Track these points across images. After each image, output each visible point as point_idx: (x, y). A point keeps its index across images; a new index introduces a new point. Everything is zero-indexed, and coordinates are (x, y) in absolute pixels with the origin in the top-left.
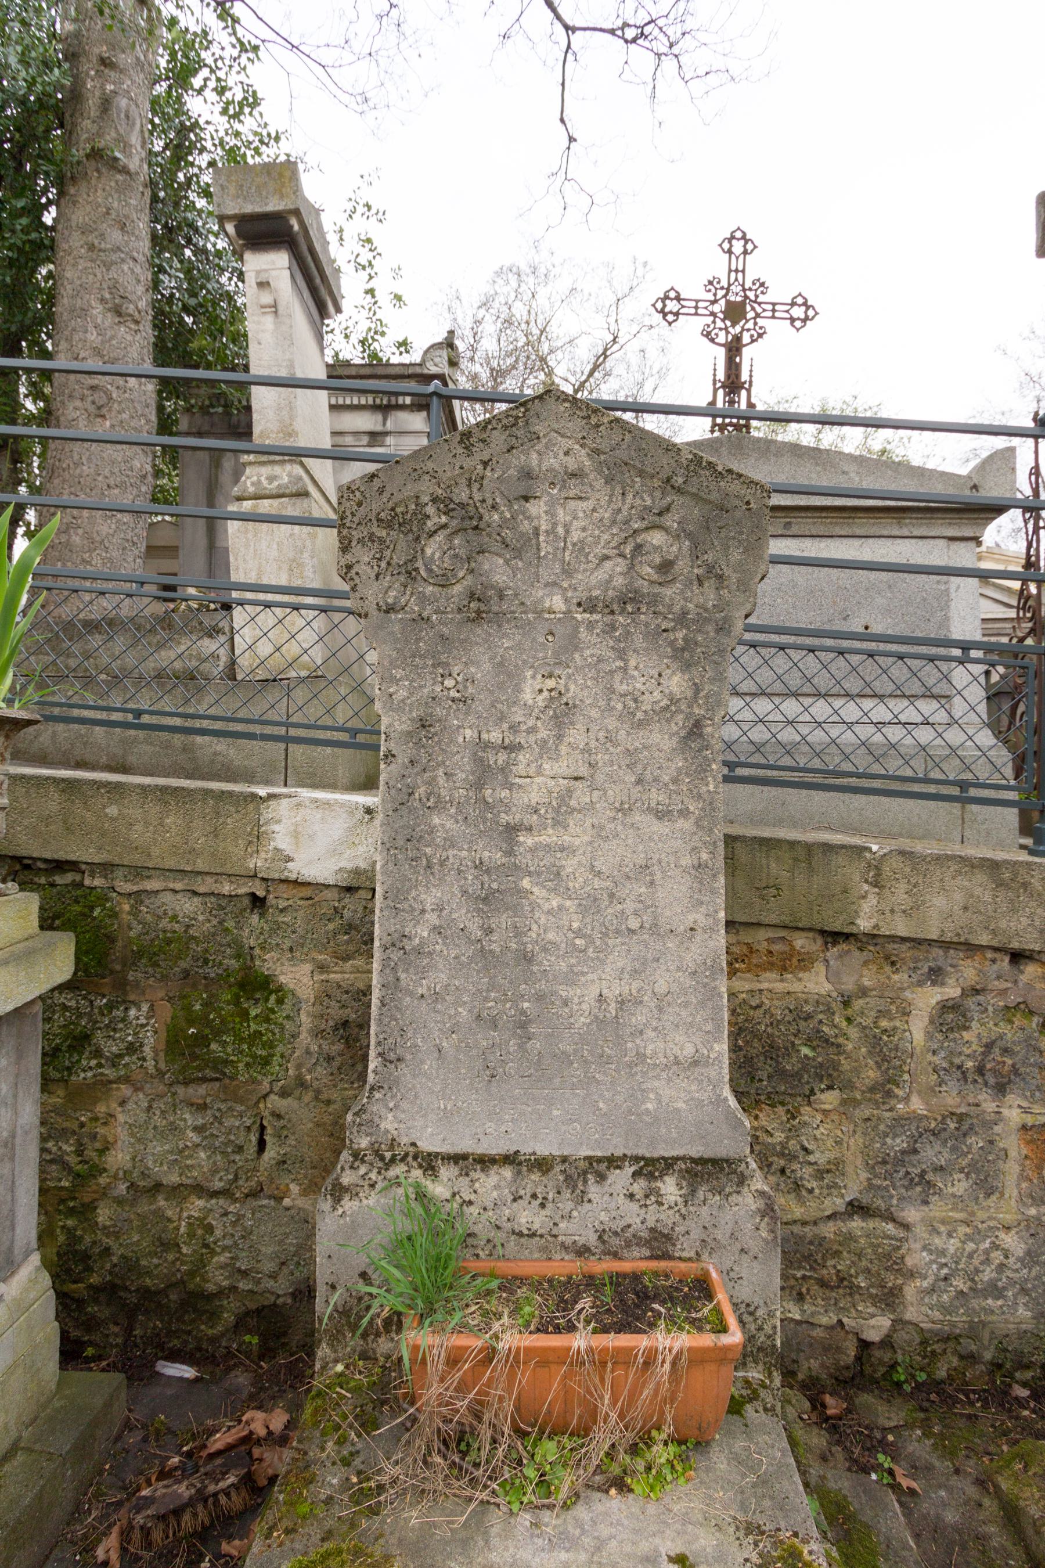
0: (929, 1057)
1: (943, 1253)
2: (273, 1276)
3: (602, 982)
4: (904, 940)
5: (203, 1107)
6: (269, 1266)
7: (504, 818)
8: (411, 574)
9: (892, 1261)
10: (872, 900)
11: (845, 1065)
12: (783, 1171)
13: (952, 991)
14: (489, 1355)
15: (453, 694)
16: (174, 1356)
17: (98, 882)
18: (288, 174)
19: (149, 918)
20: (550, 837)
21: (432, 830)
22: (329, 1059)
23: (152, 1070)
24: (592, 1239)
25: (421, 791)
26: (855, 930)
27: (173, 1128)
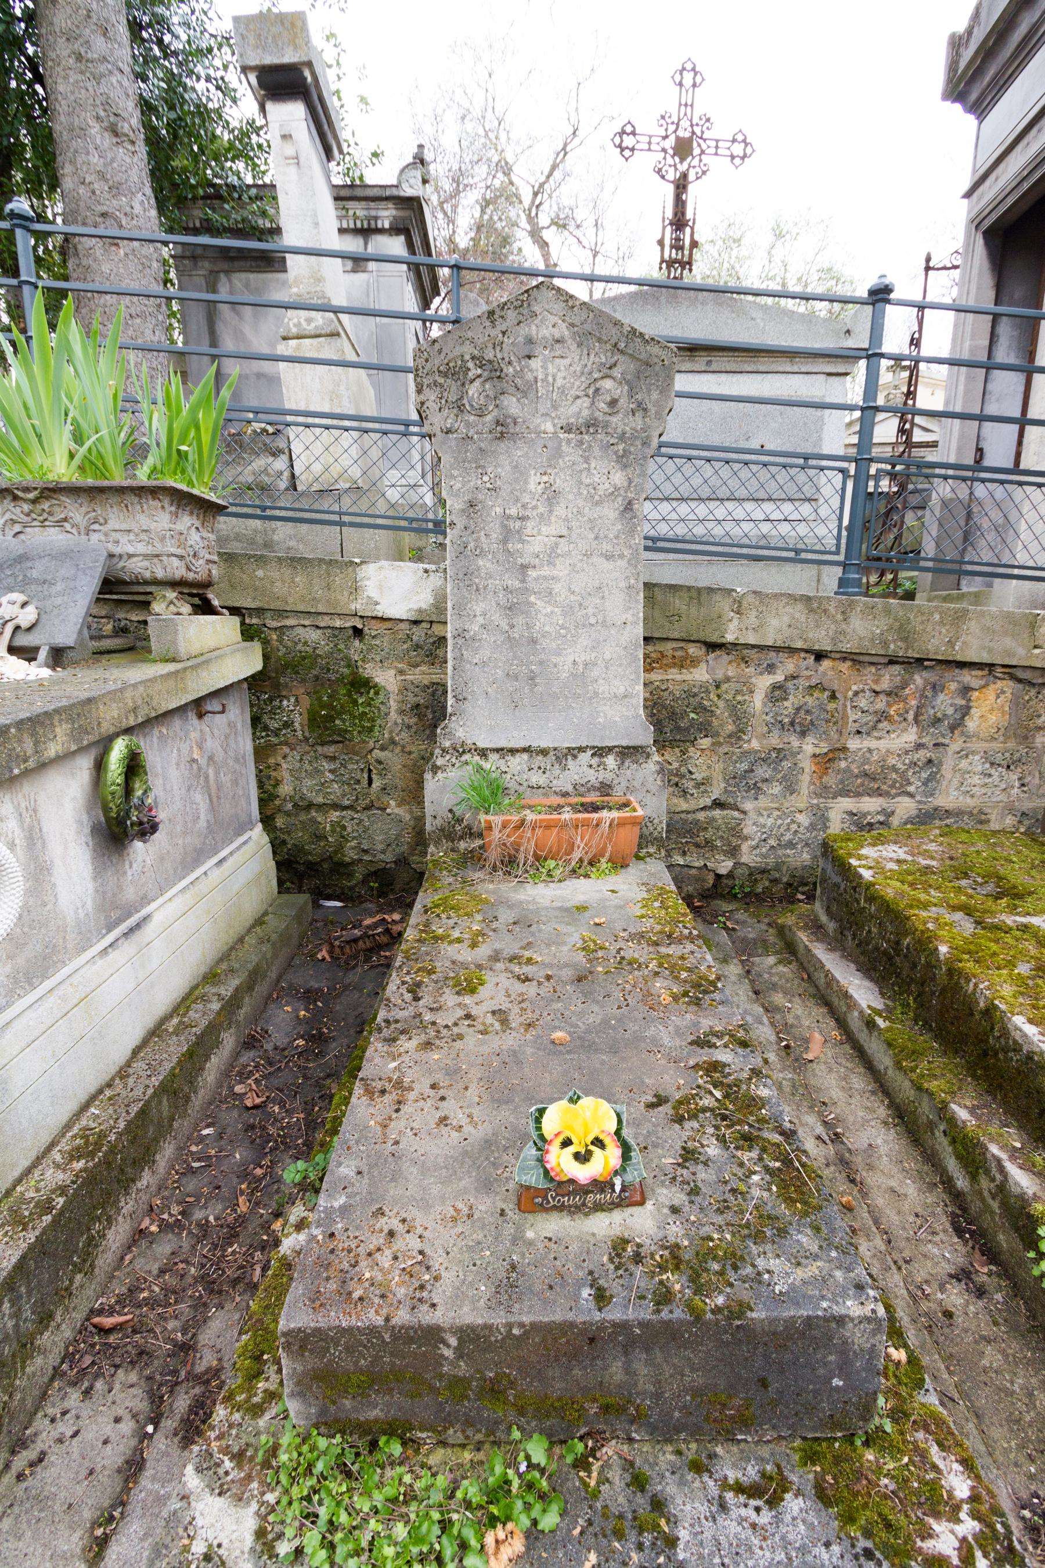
0: (764, 717)
1: (764, 826)
2: (383, 852)
3: (576, 653)
4: (753, 646)
5: (333, 759)
6: (380, 847)
7: (520, 561)
8: (461, 408)
9: (736, 831)
10: (736, 622)
11: (715, 723)
12: (677, 785)
13: (779, 677)
14: (522, 822)
15: (488, 485)
16: (329, 898)
17: (255, 621)
18: (299, 24)
19: (289, 644)
20: (546, 571)
21: (478, 569)
22: (409, 727)
23: (301, 737)
24: (569, 788)
25: (472, 545)
26: (724, 641)
27: (317, 771)
